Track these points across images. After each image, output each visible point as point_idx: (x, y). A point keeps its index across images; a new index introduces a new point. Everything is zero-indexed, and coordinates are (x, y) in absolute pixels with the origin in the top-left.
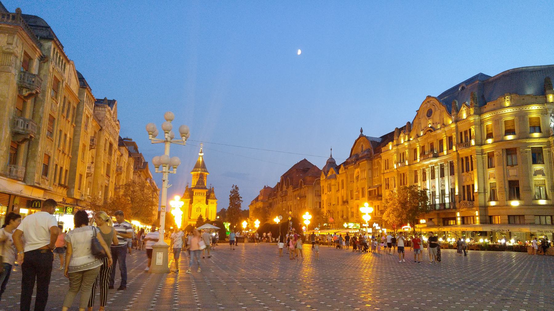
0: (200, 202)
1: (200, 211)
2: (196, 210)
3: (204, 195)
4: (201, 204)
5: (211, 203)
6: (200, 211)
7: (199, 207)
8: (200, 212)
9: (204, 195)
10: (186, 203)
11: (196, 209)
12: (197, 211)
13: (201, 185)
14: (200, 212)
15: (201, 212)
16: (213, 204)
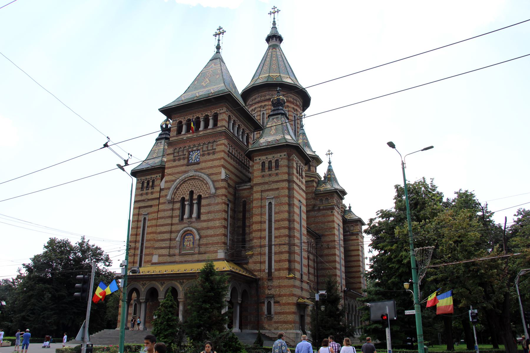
0: (196, 167)
1: (194, 215)
2: (177, 213)
3: (215, 125)
4: (197, 173)
5: (263, 164)
6: (194, 215)
7: (192, 193)
8: (199, 216)
9: (215, 125)
10: (142, 188)
11: (178, 205)
12: (182, 219)
13: (204, 87)
14: (199, 216)
15: (203, 217)
16: (274, 171)
